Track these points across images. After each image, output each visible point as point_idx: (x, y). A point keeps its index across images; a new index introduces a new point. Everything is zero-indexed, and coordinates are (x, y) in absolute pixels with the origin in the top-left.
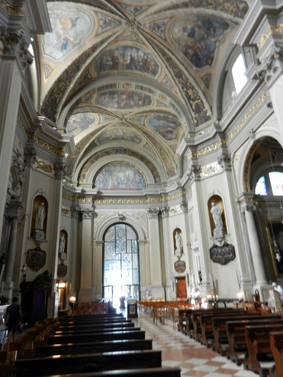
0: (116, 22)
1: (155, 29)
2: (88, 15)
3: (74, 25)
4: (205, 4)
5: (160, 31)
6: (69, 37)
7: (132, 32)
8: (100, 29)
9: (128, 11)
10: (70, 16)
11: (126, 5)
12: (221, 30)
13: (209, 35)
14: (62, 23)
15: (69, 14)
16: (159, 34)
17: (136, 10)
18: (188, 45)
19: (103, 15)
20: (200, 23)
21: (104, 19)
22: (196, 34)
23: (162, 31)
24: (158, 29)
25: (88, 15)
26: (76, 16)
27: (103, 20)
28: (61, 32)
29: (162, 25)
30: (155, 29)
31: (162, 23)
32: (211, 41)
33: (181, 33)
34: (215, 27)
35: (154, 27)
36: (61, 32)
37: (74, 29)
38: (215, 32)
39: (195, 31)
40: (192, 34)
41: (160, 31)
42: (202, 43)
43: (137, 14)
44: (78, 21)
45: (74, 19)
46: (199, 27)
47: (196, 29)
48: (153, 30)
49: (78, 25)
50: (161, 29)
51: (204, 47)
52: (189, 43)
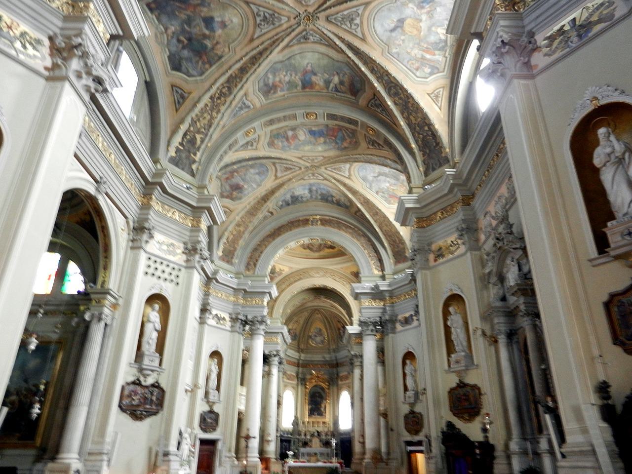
0: (333, 21)
1: (271, 15)
2: (377, 34)
3: (401, 21)
4: (224, 90)
5: (262, 14)
6: (413, 8)
7: (307, 6)
8: (360, 12)
9: (318, 36)
10: (403, 37)
11: (321, 44)
12: (174, 49)
13: (183, 31)
14: (419, 30)
15: (403, 40)
16: (261, 9)
17: (306, 38)
18: (204, 6)
19: (354, 32)
20: (208, 43)
21: (353, 27)
22: (203, 24)
23: (259, 16)
24: (265, 17)
25: (377, 34)
26: (394, 34)
27: (355, 25)
28: (424, 17)
29: (261, 24)
30: (271, 15)
31: (262, 27)
32: (172, 25)
33: (226, 19)
34: (184, 48)
35: (273, 19)
36: (424, 17)
37: (403, 16)
38: (179, 41)
39: (207, 28)
40: (209, 21)
41: (262, 14)
42: (183, 16)
43: (304, 33)
44: (393, 25)
45: (399, 30)
46: (205, 36)
47: (207, 32)
48: (274, 14)
49: (395, 20)
50: (261, 18)
51: (177, 13)
52: (205, 9)
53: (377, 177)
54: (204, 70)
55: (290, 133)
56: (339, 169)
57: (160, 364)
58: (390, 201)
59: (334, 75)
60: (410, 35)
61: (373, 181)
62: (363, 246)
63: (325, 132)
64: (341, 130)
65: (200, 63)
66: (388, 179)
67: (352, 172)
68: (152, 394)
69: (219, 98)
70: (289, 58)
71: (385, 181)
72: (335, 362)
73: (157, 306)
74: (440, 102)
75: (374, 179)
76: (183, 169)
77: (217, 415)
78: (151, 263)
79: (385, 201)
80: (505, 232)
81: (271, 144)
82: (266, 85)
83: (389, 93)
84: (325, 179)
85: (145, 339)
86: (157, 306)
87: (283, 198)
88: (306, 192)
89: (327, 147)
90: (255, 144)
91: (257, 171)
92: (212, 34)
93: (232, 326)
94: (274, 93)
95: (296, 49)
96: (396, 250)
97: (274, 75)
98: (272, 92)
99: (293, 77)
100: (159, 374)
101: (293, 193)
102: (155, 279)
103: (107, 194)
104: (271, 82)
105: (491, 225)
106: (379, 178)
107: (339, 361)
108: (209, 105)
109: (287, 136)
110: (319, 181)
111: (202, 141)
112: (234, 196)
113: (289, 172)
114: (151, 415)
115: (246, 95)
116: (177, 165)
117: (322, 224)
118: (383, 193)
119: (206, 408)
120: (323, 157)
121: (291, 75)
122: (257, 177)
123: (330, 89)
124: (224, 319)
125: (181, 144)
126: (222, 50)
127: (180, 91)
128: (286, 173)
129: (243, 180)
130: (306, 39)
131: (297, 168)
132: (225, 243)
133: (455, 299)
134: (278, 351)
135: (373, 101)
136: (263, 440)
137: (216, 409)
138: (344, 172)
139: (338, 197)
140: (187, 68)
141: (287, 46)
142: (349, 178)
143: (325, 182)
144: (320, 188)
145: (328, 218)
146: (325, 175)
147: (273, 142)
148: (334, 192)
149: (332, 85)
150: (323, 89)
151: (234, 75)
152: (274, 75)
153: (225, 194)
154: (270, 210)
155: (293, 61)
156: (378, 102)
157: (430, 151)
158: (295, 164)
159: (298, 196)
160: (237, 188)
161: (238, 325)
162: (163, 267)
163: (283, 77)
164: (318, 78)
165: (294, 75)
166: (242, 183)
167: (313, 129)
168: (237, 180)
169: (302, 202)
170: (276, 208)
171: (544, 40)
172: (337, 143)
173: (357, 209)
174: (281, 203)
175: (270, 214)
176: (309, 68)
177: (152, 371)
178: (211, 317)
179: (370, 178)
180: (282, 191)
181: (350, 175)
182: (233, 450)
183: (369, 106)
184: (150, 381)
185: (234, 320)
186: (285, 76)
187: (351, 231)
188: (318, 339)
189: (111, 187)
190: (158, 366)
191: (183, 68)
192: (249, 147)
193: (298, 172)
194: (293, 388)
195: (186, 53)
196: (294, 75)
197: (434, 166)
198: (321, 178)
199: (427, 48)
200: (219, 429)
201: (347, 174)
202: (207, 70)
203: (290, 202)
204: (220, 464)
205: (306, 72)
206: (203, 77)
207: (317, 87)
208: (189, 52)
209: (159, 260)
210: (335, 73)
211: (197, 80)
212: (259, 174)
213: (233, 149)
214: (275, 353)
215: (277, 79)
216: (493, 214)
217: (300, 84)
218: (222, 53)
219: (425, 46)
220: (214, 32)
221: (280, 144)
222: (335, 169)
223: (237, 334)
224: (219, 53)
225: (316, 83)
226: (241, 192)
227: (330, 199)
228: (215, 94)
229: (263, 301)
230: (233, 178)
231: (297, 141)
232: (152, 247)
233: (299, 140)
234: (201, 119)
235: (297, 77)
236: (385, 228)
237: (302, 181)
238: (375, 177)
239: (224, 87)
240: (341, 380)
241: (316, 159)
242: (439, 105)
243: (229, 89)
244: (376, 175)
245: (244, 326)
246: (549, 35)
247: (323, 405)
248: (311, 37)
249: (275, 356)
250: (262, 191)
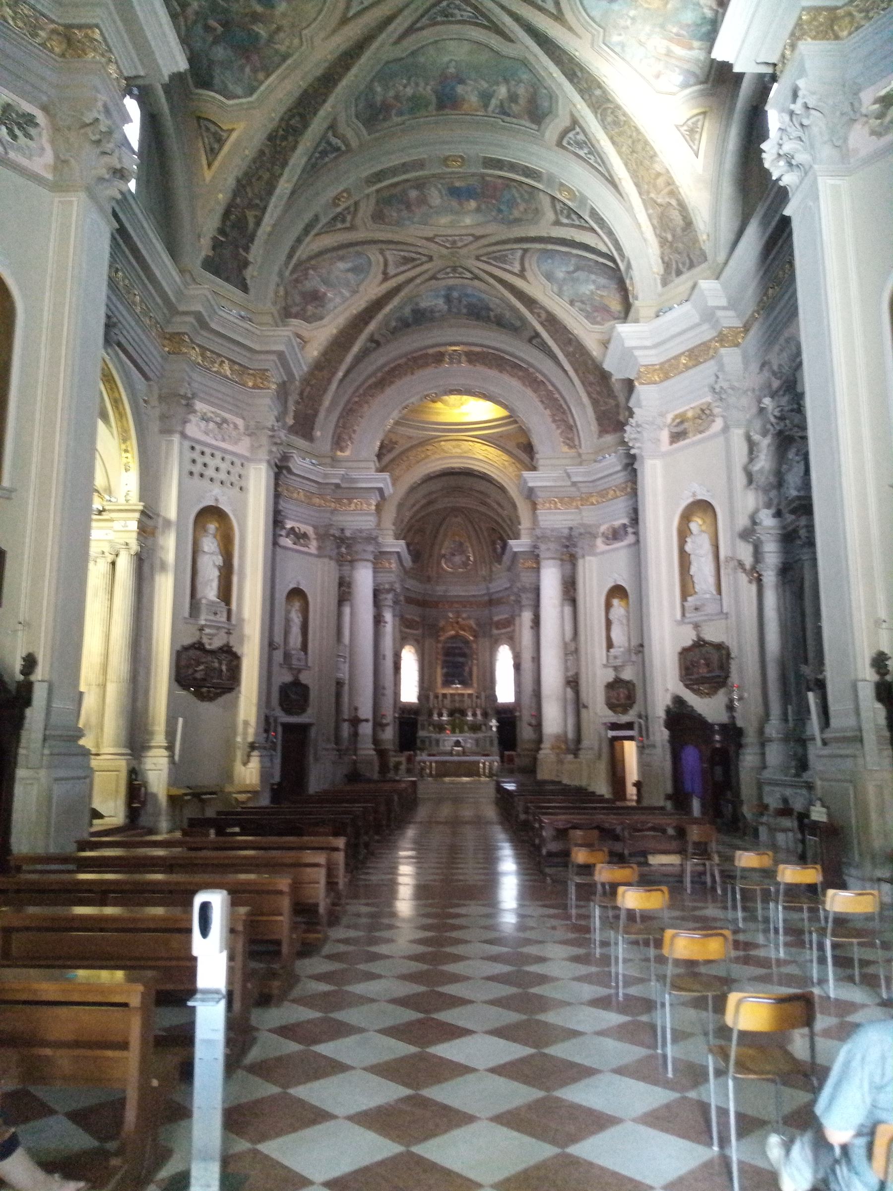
4: (292, 122)
9: (469, 9)
10: (632, 13)
15: (633, 19)
20: (261, 30)
34: (216, 42)
38: (207, 28)
46: (255, 18)
47: (259, 9)
53: (574, 272)
54: (255, 84)
55: (413, 194)
56: (503, 259)
57: (229, 618)
58: (594, 318)
59: (497, 83)
60: (647, 9)
61: (564, 279)
62: (542, 402)
64: (508, 186)
65: (248, 70)
66: (593, 277)
67: (527, 265)
68: (220, 664)
69: (285, 138)
70: (413, 53)
71: (587, 281)
72: (486, 598)
73: (212, 527)
74: (696, 142)
76: (227, 280)
77: (306, 688)
78: (196, 455)
80: (790, 407)
81: (378, 217)
82: (371, 105)
83: (603, 121)
84: (476, 277)
85: (200, 579)
86: (212, 527)
87: (398, 314)
88: (441, 301)
89: (480, 218)
90: (349, 218)
91: (349, 265)
92: (268, 12)
93: (319, 548)
94: (385, 120)
95: (428, 35)
97: (386, 88)
98: (381, 117)
99: (421, 89)
100: (229, 633)
101: (417, 304)
102: (206, 483)
103: (119, 345)
104: (379, 99)
105: (770, 386)
106: (576, 275)
107: (494, 597)
108: (267, 151)
110: (466, 281)
111: (258, 223)
112: (309, 313)
113: (409, 266)
114: (223, 693)
115: (332, 127)
116: (217, 273)
117: (470, 361)
118: (583, 302)
119: (288, 678)
120: (472, 235)
121: (417, 85)
122: (350, 276)
123: (490, 109)
124: (305, 536)
125: (222, 231)
126: (287, 43)
127: (213, 128)
130: (446, 16)
131: (424, 259)
133: (702, 507)
134: (391, 583)
135: (571, 135)
136: (378, 725)
137: (304, 678)
138: (511, 264)
139: (499, 311)
140: (223, 82)
141: (411, 30)
142: (522, 275)
143: (476, 283)
144: (467, 295)
145: (478, 349)
146: (476, 271)
147: (381, 211)
148: (494, 302)
149: (494, 102)
150: (477, 110)
151: (310, 91)
152: (386, 88)
153: (294, 310)
154: (376, 337)
155: (422, 59)
156: (581, 137)
157: (674, 236)
158: (420, 250)
159: (425, 310)
160: (315, 297)
161: (330, 545)
162: (217, 461)
163: (401, 88)
164: (469, 89)
165: (422, 84)
166: (323, 289)
168: (313, 282)
169: (432, 320)
170: (384, 331)
171: (874, 103)
172: (500, 211)
173: (533, 334)
174: (394, 324)
175: (374, 345)
176: (452, 70)
177: (218, 628)
178: (283, 533)
180: (396, 302)
181: (523, 269)
182: (333, 738)
183: (565, 143)
184: (216, 643)
185: (322, 537)
186: (405, 87)
187: (520, 373)
188: (457, 559)
189: (125, 332)
190: (224, 619)
191: (217, 81)
192: (340, 226)
194: (417, 641)
195: (220, 53)
196: (422, 84)
197: (680, 266)
198: (469, 275)
199: (677, 35)
200: (310, 711)
201: (517, 268)
202: (261, 83)
203: (410, 320)
204: (317, 760)
205: (446, 78)
206: (255, 96)
207: (466, 106)
208: (225, 48)
209: (208, 451)
210: (500, 79)
211: (241, 104)
212: (352, 270)
213: (313, 233)
214: (387, 586)
215: (391, 93)
216: (775, 368)
217: (434, 99)
218: (289, 47)
219: (675, 30)
220: (273, 7)
221: (395, 214)
222: (495, 259)
223: (326, 560)
224: (282, 48)
225: (464, 100)
226: (323, 306)
227: (484, 313)
228: (277, 131)
229: (369, 505)
231: (424, 208)
232: (194, 429)
233: (431, 207)
234: (254, 180)
235: (429, 88)
237: (433, 282)
238: (568, 273)
239: (293, 116)
240: (498, 628)
241: (461, 240)
242: (695, 148)
243: (302, 116)
244: (571, 268)
245: (339, 547)
246: (883, 93)
247: (467, 669)
248: (456, 11)
249: (388, 591)
250: (359, 304)
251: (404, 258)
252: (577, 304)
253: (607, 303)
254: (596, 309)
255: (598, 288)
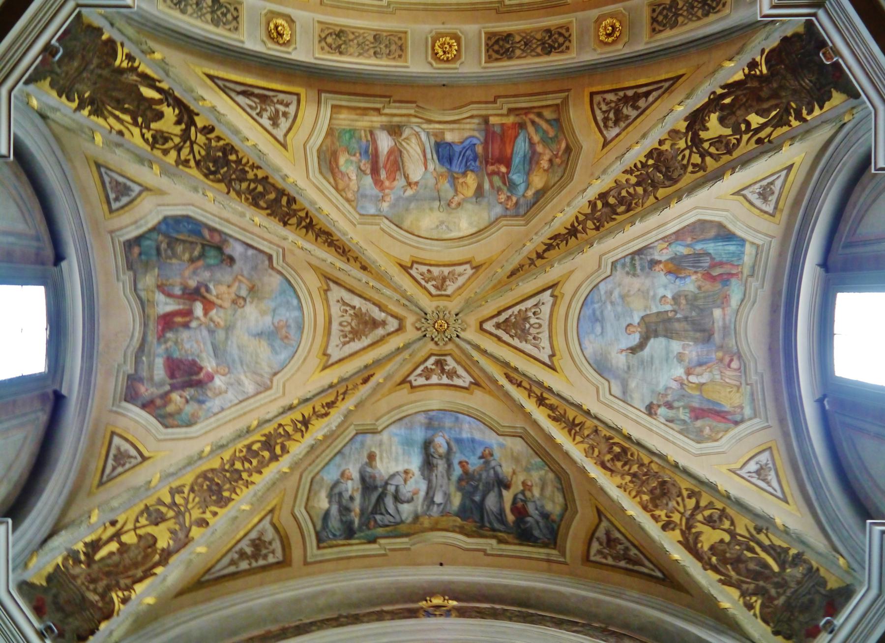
53: (641, 346)
58: (701, 430)
63: (479, 149)
66: (676, 346)
75: (634, 360)
79: (680, 432)
88: (415, 463)
96: (781, 601)
106: (647, 350)
109: (376, 149)
112: (170, 408)
113: (366, 341)
118: (669, 406)
122: (263, 350)
128: (356, 346)
129: (217, 352)
132: (73, 555)
143: (479, 401)
153: (146, 391)
166: (209, 364)
167: (449, 137)
179: (620, 360)
193: (397, 341)
230: (186, 326)
236: (709, 537)
238: (633, 350)
244: (635, 339)
251: (359, 315)
252: (662, 411)
253: (715, 397)
254: (698, 413)
255: (688, 373)
